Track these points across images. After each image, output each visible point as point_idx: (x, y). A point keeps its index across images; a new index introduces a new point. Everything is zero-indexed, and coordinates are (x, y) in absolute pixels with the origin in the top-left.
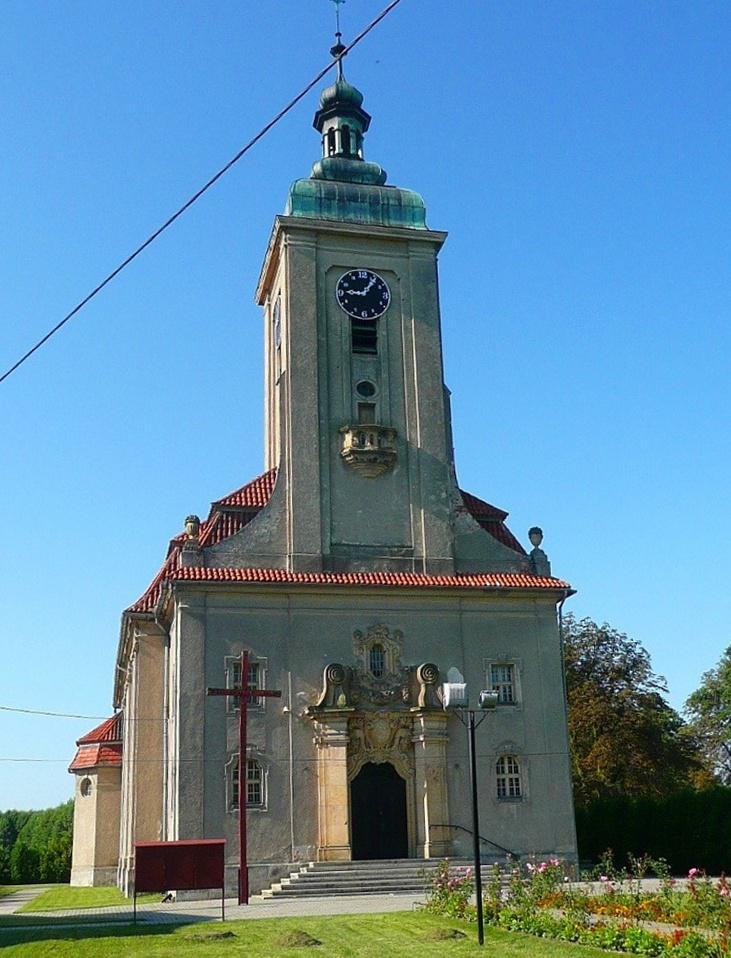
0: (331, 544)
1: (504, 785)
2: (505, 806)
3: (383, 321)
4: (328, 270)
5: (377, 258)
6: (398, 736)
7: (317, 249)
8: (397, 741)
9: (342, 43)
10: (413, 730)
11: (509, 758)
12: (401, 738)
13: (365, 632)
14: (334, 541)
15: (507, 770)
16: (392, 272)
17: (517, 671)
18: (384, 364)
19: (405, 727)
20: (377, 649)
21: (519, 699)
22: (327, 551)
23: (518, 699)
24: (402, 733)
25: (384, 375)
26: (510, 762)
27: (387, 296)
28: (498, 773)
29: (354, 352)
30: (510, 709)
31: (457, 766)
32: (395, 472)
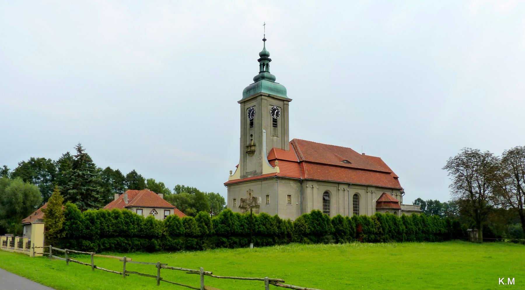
0: (246, 172)
3: (254, 119)
4: (247, 110)
5: (253, 103)
7: (244, 106)
9: (263, 41)
13: (248, 191)
14: (247, 172)
16: (255, 105)
18: (254, 129)
20: (250, 194)
22: (245, 174)
25: (254, 132)
27: (254, 112)
29: (250, 127)
32: (255, 154)
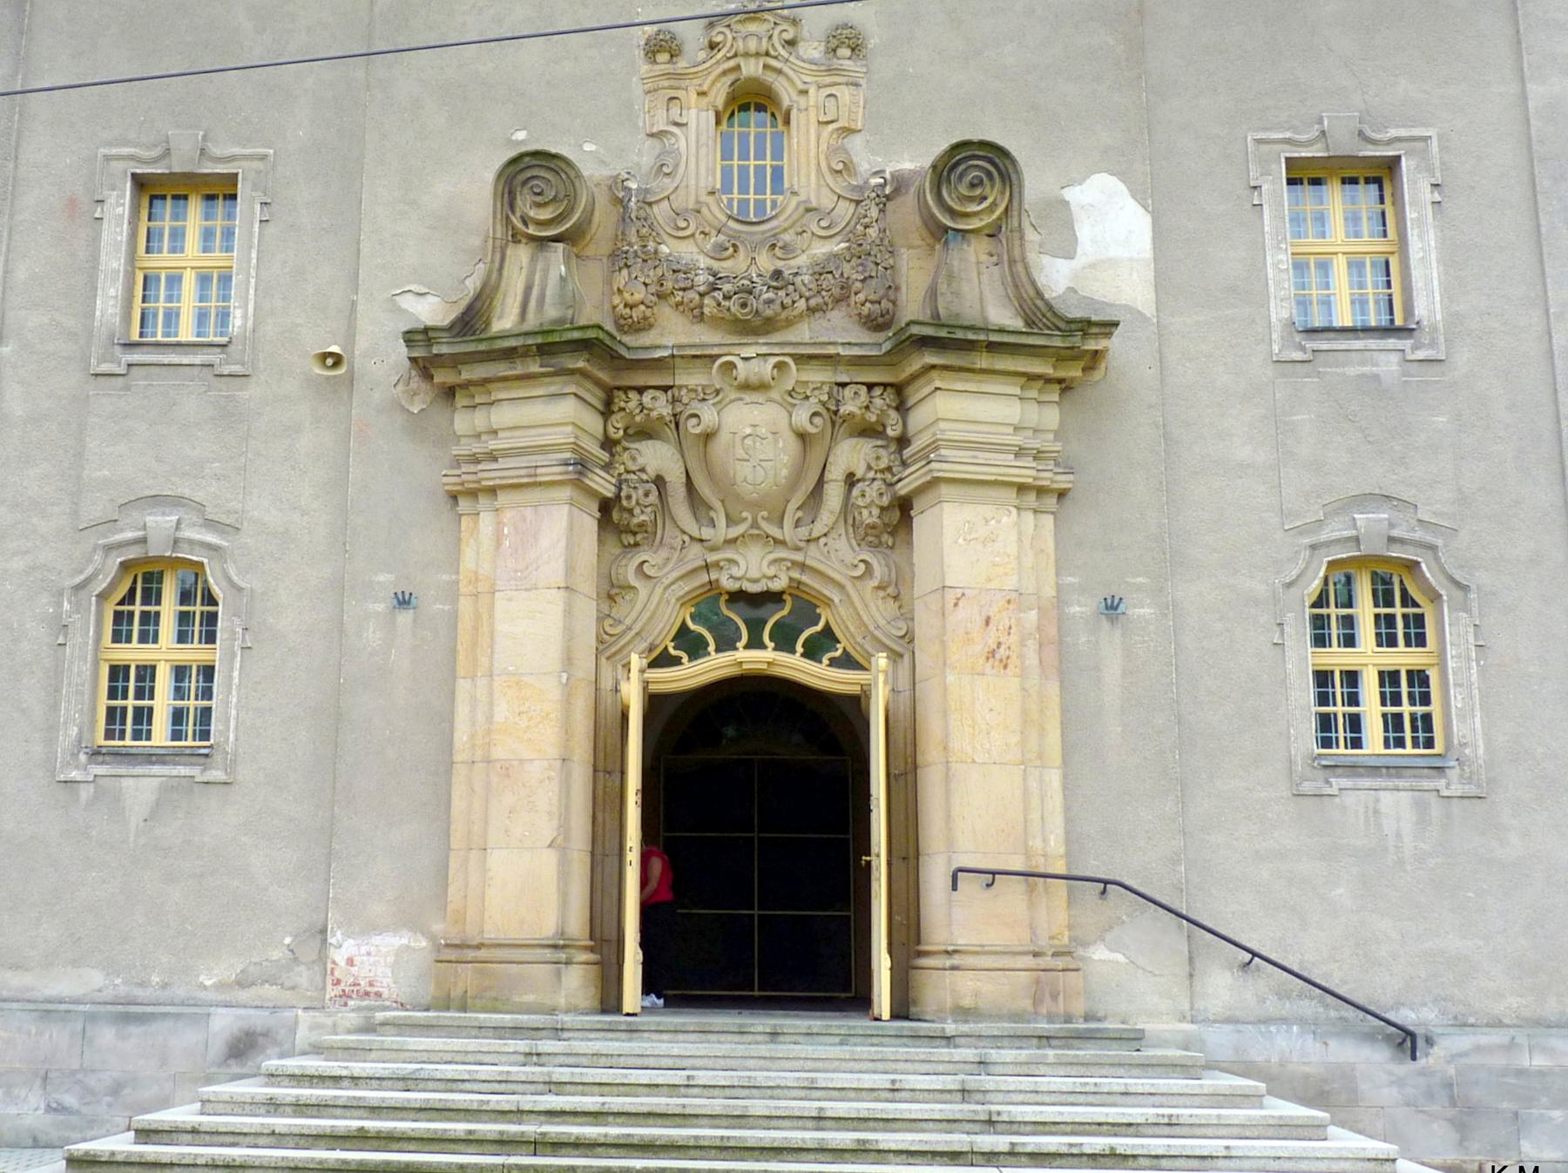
1: (1353, 700)
2: (1353, 796)
6: (836, 473)
8: (834, 495)
10: (903, 441)
11: (1375, 577)
12: (851, 480)
13: (692, 35)
15: (1366, 630)
17: (1414, 183)
19: (869, 431)
21: (1428, 305)
23: (1420, 310)
24: (852, 455)
26: (1383, 596)
28: (1320, 641)
30: (1386, 359)
31: (1112, 607)
